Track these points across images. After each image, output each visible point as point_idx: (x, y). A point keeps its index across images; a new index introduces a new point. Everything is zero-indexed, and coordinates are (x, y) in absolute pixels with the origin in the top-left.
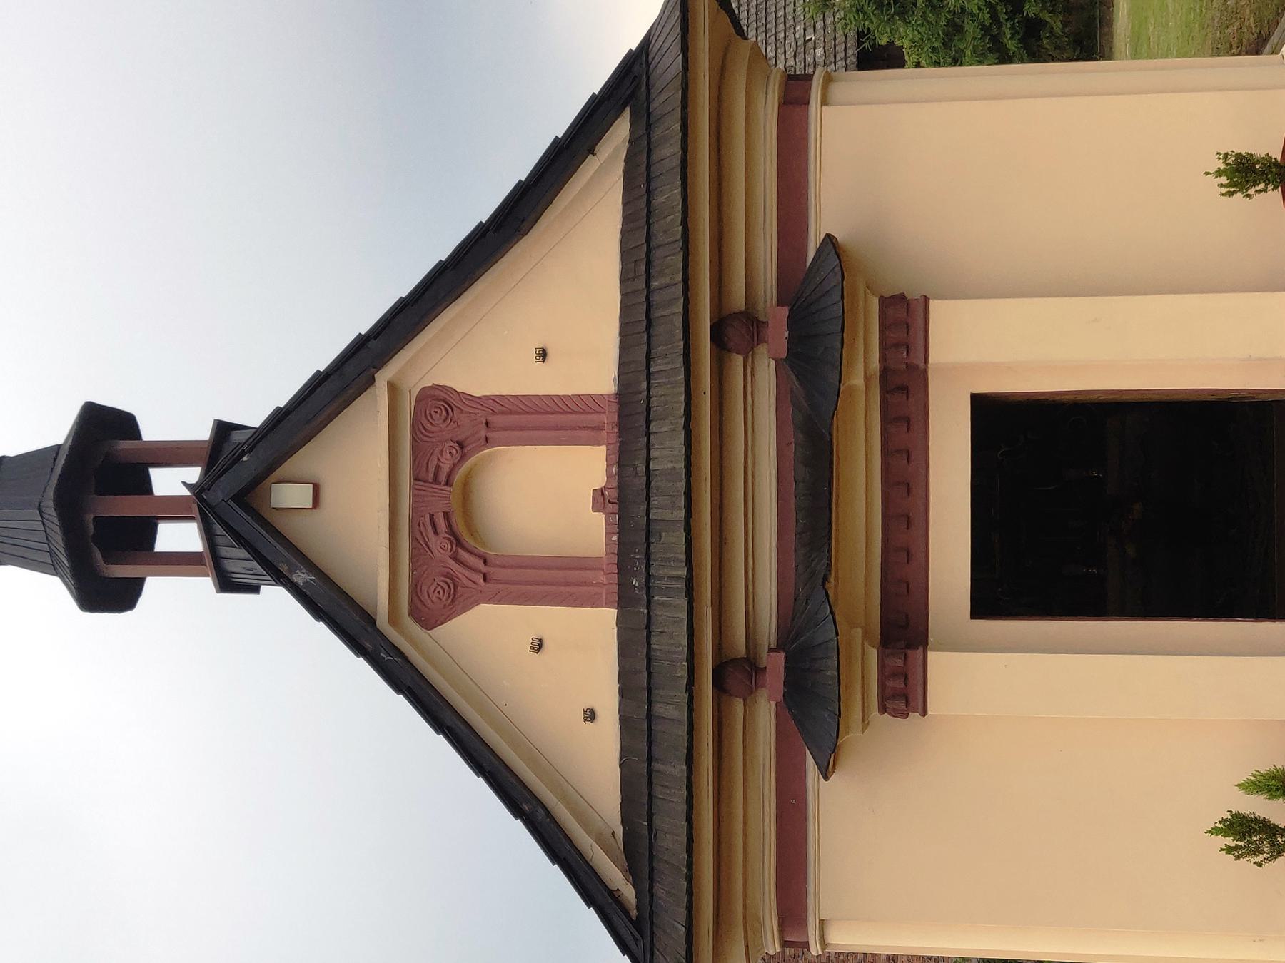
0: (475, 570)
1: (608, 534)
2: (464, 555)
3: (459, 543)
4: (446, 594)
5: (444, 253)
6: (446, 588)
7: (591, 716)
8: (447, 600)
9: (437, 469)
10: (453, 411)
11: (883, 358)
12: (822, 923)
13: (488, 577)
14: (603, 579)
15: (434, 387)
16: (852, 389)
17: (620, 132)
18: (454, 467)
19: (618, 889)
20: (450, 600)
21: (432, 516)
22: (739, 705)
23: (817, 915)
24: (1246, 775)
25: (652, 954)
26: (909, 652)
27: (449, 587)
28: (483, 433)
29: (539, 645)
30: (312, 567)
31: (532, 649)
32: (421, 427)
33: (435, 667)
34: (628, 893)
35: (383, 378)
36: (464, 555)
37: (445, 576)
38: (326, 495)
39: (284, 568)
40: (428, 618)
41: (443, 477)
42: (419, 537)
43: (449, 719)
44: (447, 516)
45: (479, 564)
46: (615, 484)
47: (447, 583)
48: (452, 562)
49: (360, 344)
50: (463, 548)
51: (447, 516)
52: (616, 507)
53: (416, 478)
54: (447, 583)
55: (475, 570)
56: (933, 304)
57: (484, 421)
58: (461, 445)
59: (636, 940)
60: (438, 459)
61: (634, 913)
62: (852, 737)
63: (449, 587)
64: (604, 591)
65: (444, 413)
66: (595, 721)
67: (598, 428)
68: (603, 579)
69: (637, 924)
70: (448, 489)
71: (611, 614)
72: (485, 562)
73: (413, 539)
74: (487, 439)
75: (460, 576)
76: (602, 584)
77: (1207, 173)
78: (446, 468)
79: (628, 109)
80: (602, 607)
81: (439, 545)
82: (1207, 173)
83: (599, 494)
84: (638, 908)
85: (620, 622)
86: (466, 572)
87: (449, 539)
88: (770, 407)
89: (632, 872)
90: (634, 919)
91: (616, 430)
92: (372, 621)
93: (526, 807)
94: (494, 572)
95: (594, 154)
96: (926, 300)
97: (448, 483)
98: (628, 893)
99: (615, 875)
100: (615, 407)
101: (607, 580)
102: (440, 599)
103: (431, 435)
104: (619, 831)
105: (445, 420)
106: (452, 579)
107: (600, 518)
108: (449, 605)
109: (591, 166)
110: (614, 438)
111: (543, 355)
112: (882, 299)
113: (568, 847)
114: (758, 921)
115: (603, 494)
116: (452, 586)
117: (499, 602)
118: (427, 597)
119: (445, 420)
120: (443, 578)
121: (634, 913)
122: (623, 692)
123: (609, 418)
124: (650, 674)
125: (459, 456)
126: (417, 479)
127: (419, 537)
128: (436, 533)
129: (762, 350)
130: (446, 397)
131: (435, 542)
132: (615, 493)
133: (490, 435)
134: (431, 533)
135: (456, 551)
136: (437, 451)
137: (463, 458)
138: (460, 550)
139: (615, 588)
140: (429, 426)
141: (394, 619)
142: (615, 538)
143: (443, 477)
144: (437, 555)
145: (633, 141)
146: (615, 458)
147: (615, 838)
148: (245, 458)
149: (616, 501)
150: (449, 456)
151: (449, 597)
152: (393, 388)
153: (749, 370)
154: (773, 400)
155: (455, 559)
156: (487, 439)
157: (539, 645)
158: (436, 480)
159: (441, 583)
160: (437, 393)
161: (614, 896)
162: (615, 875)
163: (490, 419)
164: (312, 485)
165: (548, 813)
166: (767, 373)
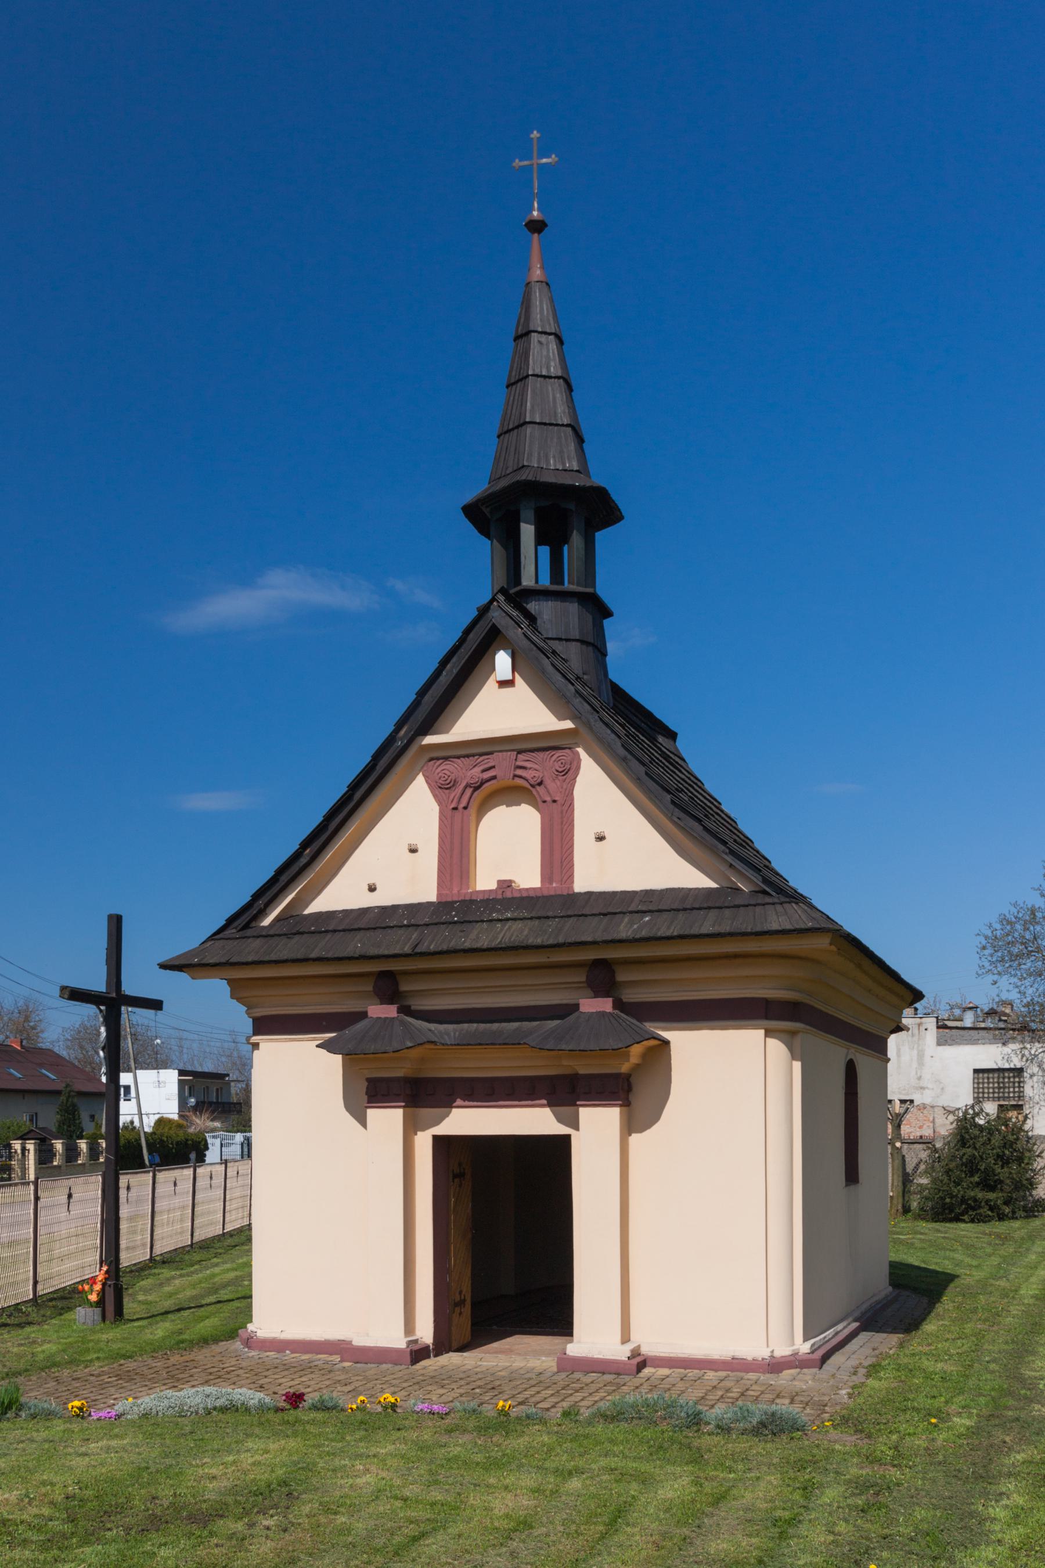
2: (469, 791)
3: (476, 789)
6: (448, 781)
7: (372, 889)
21: (494, 767)
31: (410, 845)
37: (455, 781)
41: (519, 772)
45: (463, 804)
48: (464, 784)
51: (494, 778)
52: (500, 897)
65: (560, 770)
71: (432, 896)
72: (465, 808)
85: (429, 904)
86: (458, 795)
94: (458, 815)
101: (455, 894)
105: (557, 771)
106: (453, 785)
107: (493, 886)
110: (546, 893)
111: (600, 838)
117: (440, 819)
119: (557, 771)
122: (384, 909)
124: (393, 927)
125: (532, 782)
128: (484, 771)
132: (508, 895)
134: (482, 768)
136: (536, 766)
138: (472, 789)
139: (449, 899)
143: (519, 772)
155: (466, 787)
160: (575, 763)
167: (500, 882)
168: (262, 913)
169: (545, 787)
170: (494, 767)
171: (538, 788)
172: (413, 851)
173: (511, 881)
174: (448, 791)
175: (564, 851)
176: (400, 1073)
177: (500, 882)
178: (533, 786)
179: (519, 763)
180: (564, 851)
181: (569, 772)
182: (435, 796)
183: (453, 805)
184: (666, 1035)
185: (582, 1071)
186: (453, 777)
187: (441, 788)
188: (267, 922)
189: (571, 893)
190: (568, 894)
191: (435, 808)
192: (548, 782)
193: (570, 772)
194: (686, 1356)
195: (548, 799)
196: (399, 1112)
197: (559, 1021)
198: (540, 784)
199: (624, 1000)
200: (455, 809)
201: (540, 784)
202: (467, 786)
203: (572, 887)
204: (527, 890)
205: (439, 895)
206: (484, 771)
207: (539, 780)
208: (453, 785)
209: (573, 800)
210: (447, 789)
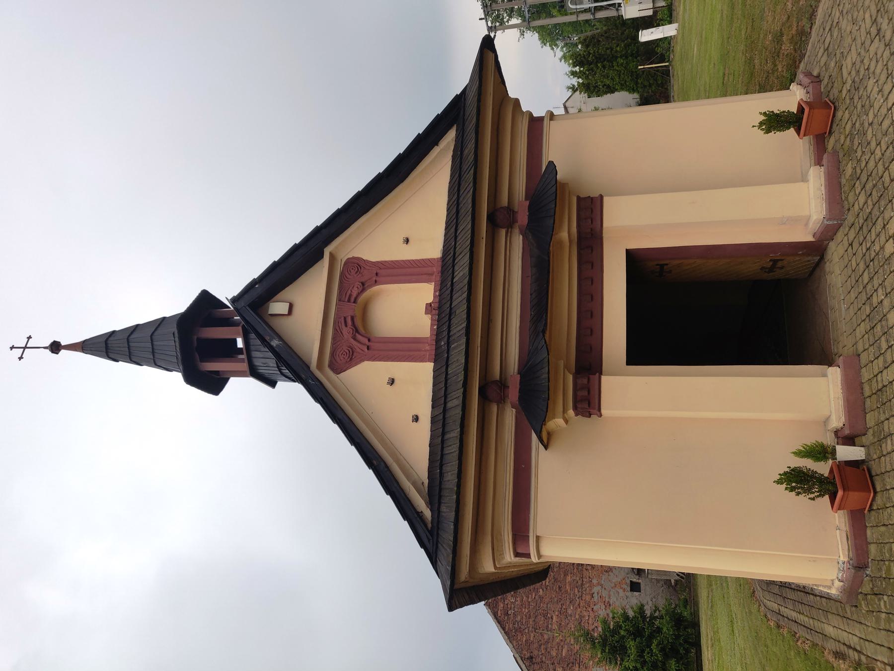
0: (364, 344)
1: (432, 325)
2: (359, 337)
3: (357, 331)
4: (348, 355)
5: (360, 187)
6: (348, 352)
7: (416, 419)
8: (348, 358)
9: (350, 296)
10: (361, 268)
11: (578, 226)
12: (538, 538)
13: (369, 347)
14: (428, 348)
15: (354, 258)
16: (560, 243)
17: (451, 135)
18: (359, 295)
19: (422, 512)
20: (349, 360)
21: (345, 318)
22: (494, 408)
23: (535, 532)
24: (798, 446)
25: (437, 547)
26: (591, 376)
27: (349, 352)
28: (374, 279)
29: (392, 382)
30: (280, 338)
32: (345, 277)
33: (338, 392)
34: (428, 513)
35: (327, 251)
36: (359, 337)
37: (349, 347)
38: (296, 310)
39: (267, 338)
40: (337, 368)
41: (352, 300)
42: (338, 328)
43: (340, 415)
44: (353, 318)
46: (437, 300)
47: (349, 350)
48: (352, 340)
49: (317, 231)
50: (359, 334)
51: (353, 318)
52: (437, 311)
53: (340, 299)
54: (349, 350)
55: (364, 344)
56: (605, 199)
57: (375, 272)
58: (363, 284)
59: (429, 541)
60: (351, 291)
61: (430, 526)
62: (556, 423)
63: (349, 352)
64: (428, 354)
65: (356, 269)
66: (418, 422)
67: (432, 274)
68: (428, 348)
69: (431, 532)
70: (354, 304)
71: (429, 366)
72: (369, 340)
73: (335, 329)
74: (376, 281)
75: (356, 347)
76: (426, 351)
77: (753, 126)
78: (354, 295)
79: (455, 125)
80: (426, 362)
81: (347, 332)
82: (753, 126)
83: (429, 306)
84: (432, 523)
86: (359, 345)
87: (352, 328)
88: (519, 257)
89: (430, 504)
90: (430, 529)
91: (440, 274)
92: (308, 367)
93: (375, 462)
95: (437, 145)
96: (601, 197)
97: (355, 302)
98: (428, 513)
99: (421, 504)
100: (440, 263)
101: (430, 348)
102: (344, 358)
103: (347, 280)
104: (426, 482)
105: (356, 273)
106: (352, 349)
108: (349, 361)
109: (436, 151)
110: (438, 278)
111: (407, 241)
112: (579, 198)
113: (396, 485)
114: (501, 535)
115: (431, 306)
116: (351, 352)
117: (374, 360)
118: (338, 357)
119: (356, 273)
120: (347, 348)
121: (430, 526)
123: (437, 269)
126: (340, 300)
127: (338, 328)
128: (346, 326)
129: (516, 231)
130: (358, 262)
131: (345, 330)
132: (437, 305)
133: (378, 279)
135: (355, 335)
137: (363, 290)
138: (357, 334)
140: (348, 276)
141: (320, 365)
142: (435, 327)
143: (352, 300)
144: (345, 336)
145: (457, 137)
146: (438, 288)
147: (423, 486)
148: (257, 286)
149: (437, 308)
150: (356, 289)
151: (349, 357)
152: (332, 257)
153: (508, 239)
154: (520, 255)
155: (355, 339)
156: (376, 281)
157: (392, 382)
158: (349, 301)
159: (346, 350)
161: (420, 515)
162: (421, 504)
163: (378, 271)
164: (289, 304)
165: (387, 466)
166: (518, 241)
167: (426, 313)
169: (366, 281)
170: (345, 318)
174: (355, 354)
175: (412, 266)
176: (570, 378)
177: (426, 313)
180: (412, 266)
182: (356, 364)
187: (352, 359)
192: (363, 280)
196: (603, 378)
200: (368, 348)
202: (354, 338)
203: (437, 258)
204: (434, 297)
206: (346, 326)
207: (360, 284)
209: (378, 262)
210: (353, 354)
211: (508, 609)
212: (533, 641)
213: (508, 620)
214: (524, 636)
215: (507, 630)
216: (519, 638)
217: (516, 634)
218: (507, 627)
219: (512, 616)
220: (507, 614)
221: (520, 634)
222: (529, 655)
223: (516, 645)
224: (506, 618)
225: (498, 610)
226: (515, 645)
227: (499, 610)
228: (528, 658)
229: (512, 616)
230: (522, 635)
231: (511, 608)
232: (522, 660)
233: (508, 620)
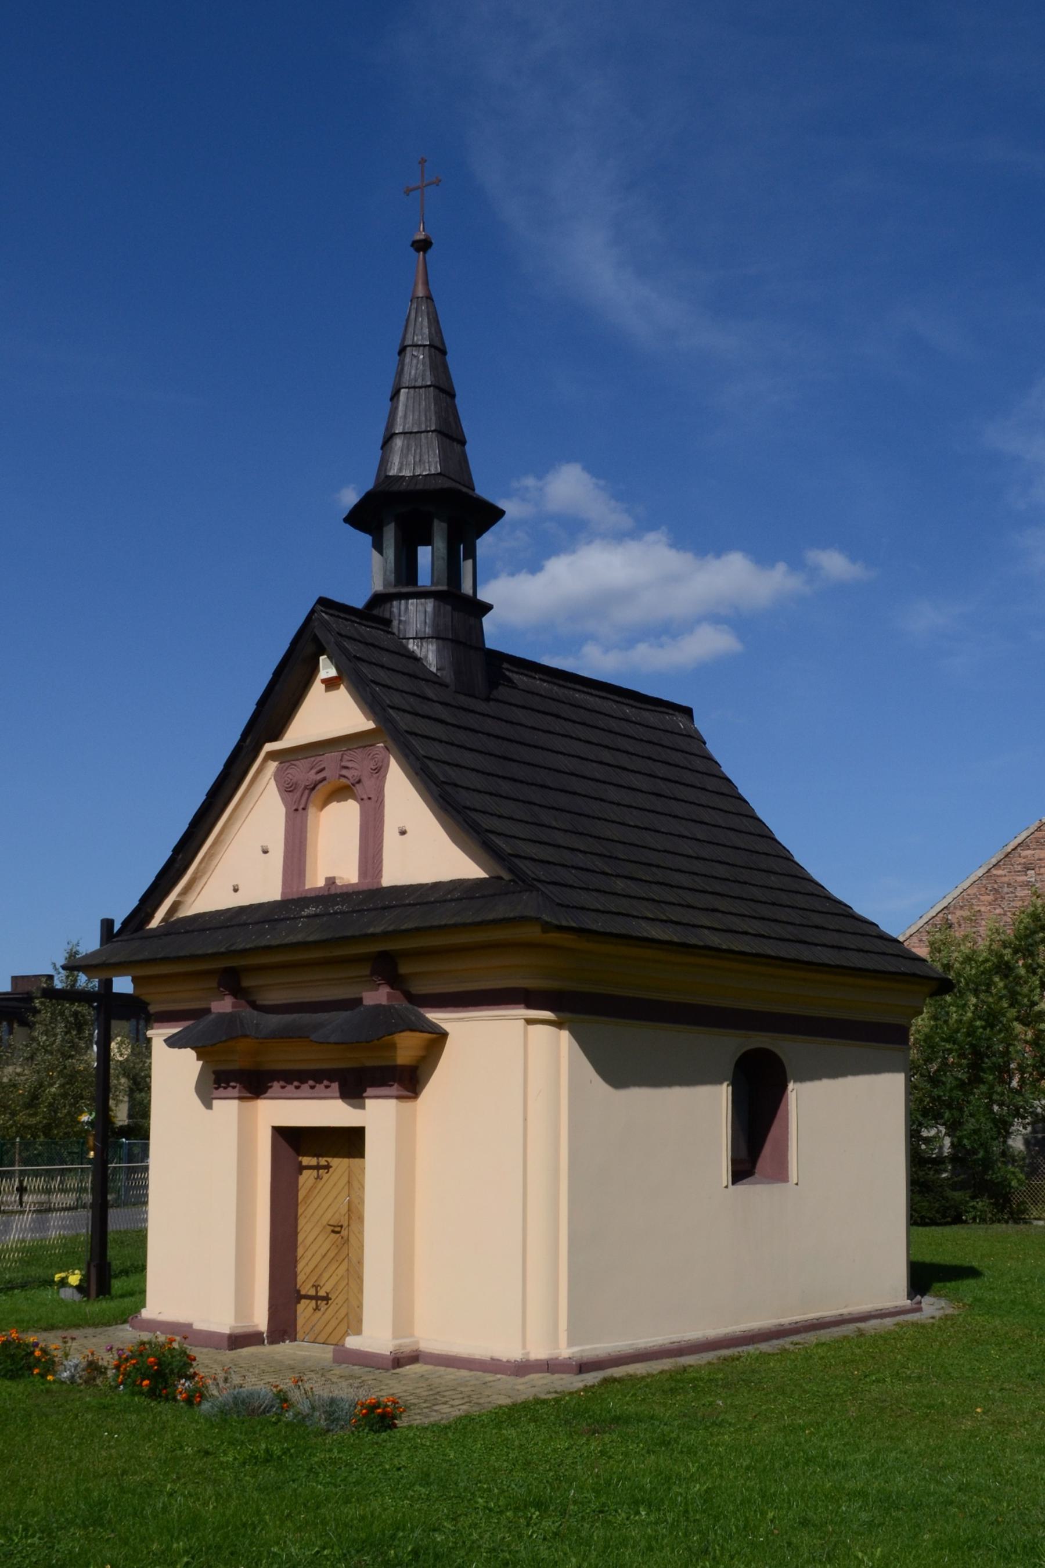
2: (307, 792)
41: (344, 772)
46: (339, 891)
51: (324, 779)
55: (299, 804)
65: (374, 768)
72: (304, 809)
111: (403, 833)
132: (333, 891)
143: (344, 772)
168: (151, 916)
171: (357, 785)
172: (265, 852)
173: (334, 878)
174: (291, 794)
178: (353, 785)
179: (344, 764)
181: (380, 771)
182: (283, 799)
183: (295, 807)
184: (446, 1026)
185: (369, 1063)
186: (294, 780)
188: (154, 923)
189: (379, 887)
190: (377, 889)
191: (282, 810)
192: (365, 780)
193: (382, 770)
194: (454, 1354)
195: (365, 797)
197: (348, 1013)
198: (359, 782)
199: (414, 992)
200: (296, 810)
201: (359, 782)
202: (306, 788)
205: (283, 893)
208: (295, 788)
209: (384, 796)
211: (1037, 869)
212: (981, 926)
213: (1015, 872)
214: (988, 908)
215: (994, 872)
216: (982, 898)
217: (991, 891)
218: (1000, 872)
219: (1025, 878)
220: (1027, 868)
221: (990, 898)
222: (955, 921)
223: (969, 895)
224: (1019, 868)
225: (1034, 849)
226: (969, 891)
227: (1033, 852)
228: (947, 919)
229: (1025, 878)
230: (990, 904)
231: (1039, 874)
232: (943, 910)
233: (1015, 872)
